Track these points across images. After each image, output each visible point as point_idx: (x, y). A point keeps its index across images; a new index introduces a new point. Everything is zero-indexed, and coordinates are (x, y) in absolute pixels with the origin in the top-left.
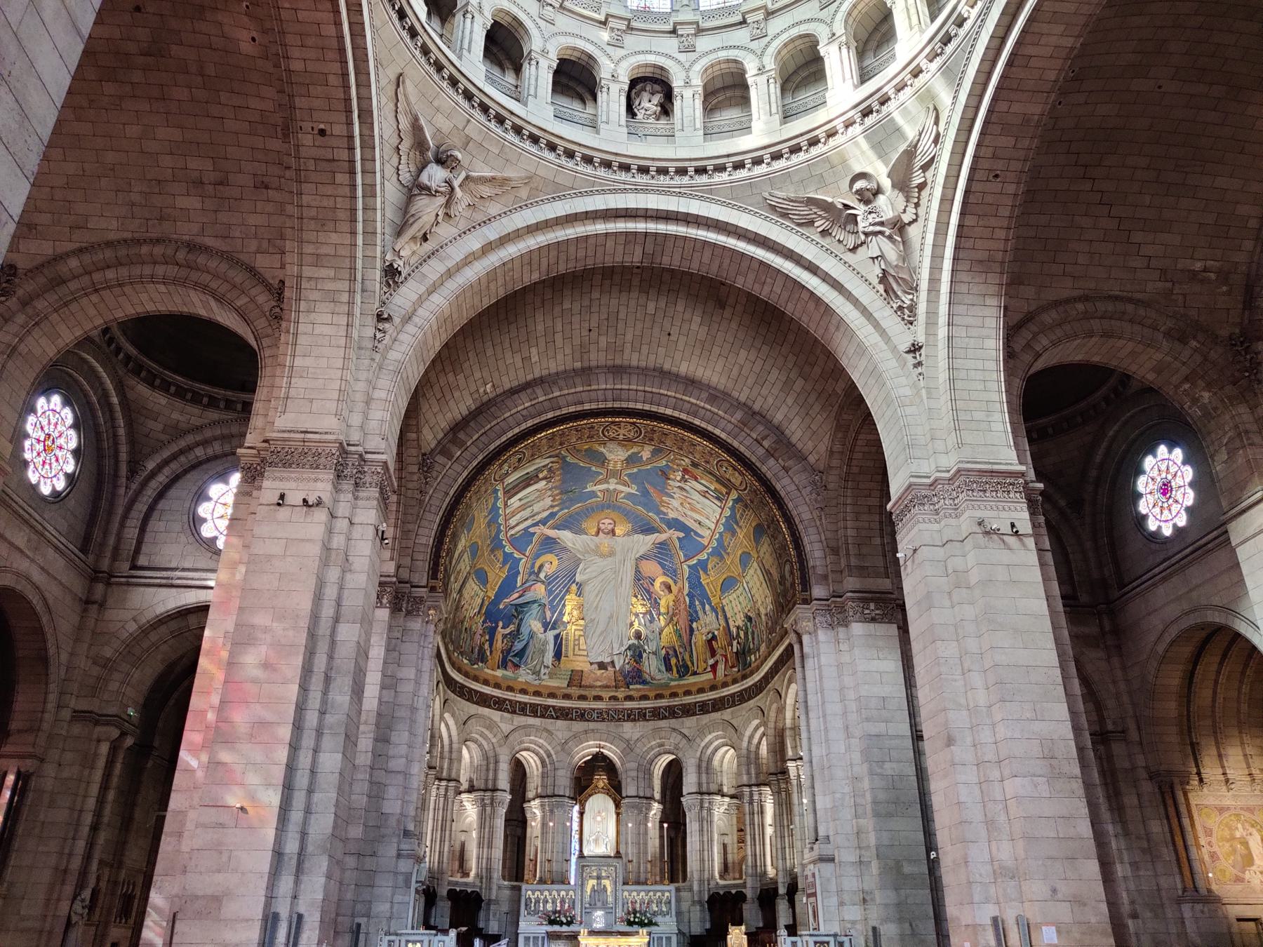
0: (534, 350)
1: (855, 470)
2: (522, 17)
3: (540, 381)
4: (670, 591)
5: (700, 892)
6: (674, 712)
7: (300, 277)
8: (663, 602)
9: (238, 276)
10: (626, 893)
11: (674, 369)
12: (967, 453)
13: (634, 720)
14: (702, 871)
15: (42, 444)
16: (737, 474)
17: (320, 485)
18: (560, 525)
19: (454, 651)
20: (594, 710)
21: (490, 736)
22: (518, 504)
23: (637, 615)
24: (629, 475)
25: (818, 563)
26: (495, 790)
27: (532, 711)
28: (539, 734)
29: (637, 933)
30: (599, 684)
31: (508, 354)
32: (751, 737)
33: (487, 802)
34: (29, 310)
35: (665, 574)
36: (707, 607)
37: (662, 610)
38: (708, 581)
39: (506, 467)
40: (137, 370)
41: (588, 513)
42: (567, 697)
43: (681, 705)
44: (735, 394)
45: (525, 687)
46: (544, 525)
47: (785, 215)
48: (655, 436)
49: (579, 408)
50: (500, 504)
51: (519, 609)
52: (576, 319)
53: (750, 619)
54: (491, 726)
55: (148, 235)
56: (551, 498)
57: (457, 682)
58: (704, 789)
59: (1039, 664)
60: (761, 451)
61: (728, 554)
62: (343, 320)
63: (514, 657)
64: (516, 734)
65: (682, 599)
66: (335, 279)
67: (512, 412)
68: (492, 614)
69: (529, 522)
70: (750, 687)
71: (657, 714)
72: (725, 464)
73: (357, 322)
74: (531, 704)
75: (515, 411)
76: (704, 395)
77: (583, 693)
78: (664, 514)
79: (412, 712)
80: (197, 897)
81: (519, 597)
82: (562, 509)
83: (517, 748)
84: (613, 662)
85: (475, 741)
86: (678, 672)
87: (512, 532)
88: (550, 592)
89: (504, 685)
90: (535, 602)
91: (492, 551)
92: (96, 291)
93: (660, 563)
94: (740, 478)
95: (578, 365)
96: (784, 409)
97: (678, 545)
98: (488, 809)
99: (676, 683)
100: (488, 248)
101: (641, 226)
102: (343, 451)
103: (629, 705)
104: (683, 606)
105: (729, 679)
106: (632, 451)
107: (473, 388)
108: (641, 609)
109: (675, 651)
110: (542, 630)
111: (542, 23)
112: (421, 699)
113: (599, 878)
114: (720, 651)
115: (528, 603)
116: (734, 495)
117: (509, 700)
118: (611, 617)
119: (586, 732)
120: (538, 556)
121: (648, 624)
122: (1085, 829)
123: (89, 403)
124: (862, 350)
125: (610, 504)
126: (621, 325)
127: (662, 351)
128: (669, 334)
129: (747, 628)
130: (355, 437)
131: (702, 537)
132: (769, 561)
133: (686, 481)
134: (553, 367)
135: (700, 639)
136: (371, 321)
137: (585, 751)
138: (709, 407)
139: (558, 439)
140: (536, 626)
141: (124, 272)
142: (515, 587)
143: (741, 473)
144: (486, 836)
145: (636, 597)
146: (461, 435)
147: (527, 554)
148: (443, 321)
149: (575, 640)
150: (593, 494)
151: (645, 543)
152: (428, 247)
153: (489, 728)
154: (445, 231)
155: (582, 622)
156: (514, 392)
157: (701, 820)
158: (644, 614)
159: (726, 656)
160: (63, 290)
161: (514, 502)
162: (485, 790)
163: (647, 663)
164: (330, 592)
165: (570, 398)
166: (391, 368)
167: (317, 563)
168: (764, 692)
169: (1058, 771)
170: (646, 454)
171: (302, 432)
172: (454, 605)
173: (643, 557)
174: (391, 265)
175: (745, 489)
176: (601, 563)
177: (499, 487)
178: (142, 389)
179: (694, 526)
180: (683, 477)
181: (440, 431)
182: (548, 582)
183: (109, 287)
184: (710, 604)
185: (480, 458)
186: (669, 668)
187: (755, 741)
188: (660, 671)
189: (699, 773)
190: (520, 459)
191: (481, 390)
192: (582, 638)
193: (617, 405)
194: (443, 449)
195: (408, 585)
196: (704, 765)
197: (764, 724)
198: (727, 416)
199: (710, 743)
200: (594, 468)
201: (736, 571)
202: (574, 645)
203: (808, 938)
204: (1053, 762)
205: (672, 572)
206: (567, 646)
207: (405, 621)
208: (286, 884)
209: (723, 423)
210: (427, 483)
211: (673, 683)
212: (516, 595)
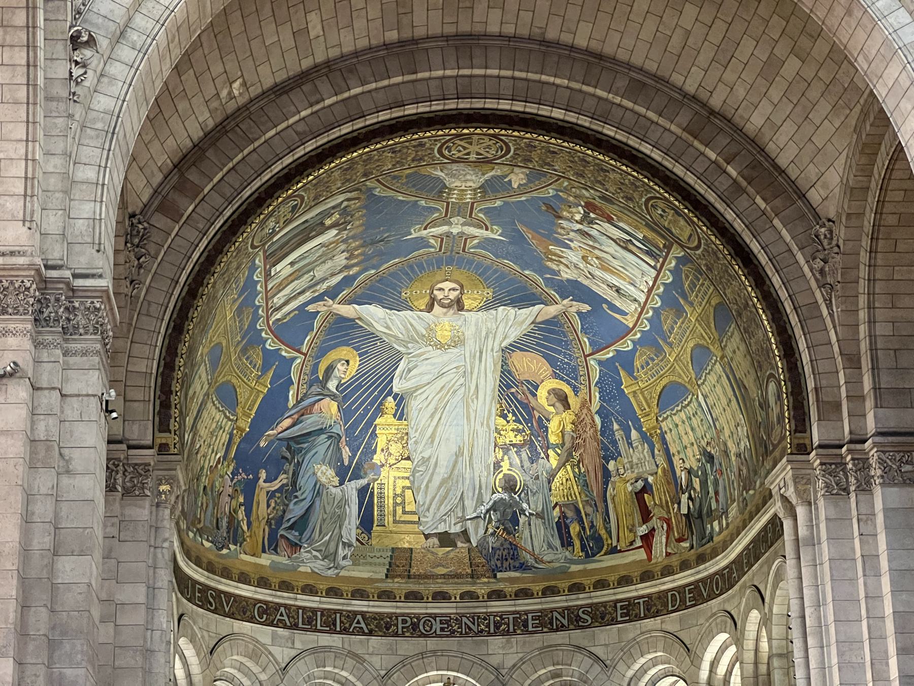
0: (313, 18)
1: (891, 220)
3: (327, 68)
8: (553, 426)
11: (566, 38)
13: (507, 633)
16: (682, 222)
17: (11, 341)
18: (360, 297)
19: (188, 528)
20: (434, 616)
21: (256, 669)
22: (289, 270)
23: (506, 449)
24: (487, 211)
25: (824, 383)
28: (340, 663)
30: (442, 571)
32: (714, 664)
35: (556, 376)
36: (634, 434)
37: (553, 439)
38: (636, 388)
39: (271, 223)
41: (412, 273)
42: (386, 595)
43: (590, 605)
44: (677, 79)
45: (311, 582)
46: (333, 298)
48: (535, 156)
49: (397, 113)
50: (258, 276)
51: (294, 446)
53: (710, 458)
54: (257, 652)
57: (196, 582)
60: (723, 184)
61: (670, 345)
62: (20, 57)
64: (300, 664)
65: (588, 420)
67: (280, 128)
69: (308, 295)
70: (711, 577)
72: (660, 204)
74: (323, 611)
75: (284, 125)
77: (413, 587)
79: (145, 658)
81: (293, 425)
82: (366, 270)
84: (465, 533)
86: (583, 547)
87: (278, 316)
88: (346, 413)
89: (275, 581)
90: (321, 431)
93: (546, 356)
94: (688, 231)
95: (392, 36)
96: (765, 108)
99: (580, 567)
102: (44, 283)
103: (497, 606)
104: (590, 432)
105: (675, 561)
107: (210, 91)
108: (511, 437)
109: (578, 511)
110: (336, 480)
112: (157, 634)
114: (657, 512)
115: (309, 434)
116: (676, 252)
117: (286, 606)
118: (459, 454)
119: (422, 655)
120: (323, 352)
121: (527, 464)
124: (890, 51)
129: (705, 473)
130: (56, 253)
131: (623, 313)
132: (742, 365)
133: (591, 222)
136: (61, 49)
138: (630, 105)
139: (360, 169)
140: (326, 474)
142: (287, 409)
143: (690, 222)
145: (505, 417)
146: (193, 176)
150: (422, 243)
153: (254, 656)
155: (407, 464)
156: (280, 90)
159: (668, 521)
161: (283, 268)
163: (526, 533)
165: (380, 97)
166: (99, 125)
167: (21, 469)
168: (736, 587)
173: (515, 346)
175: (698, 247)
176: (437, 358)
177: (261, 253)
179: (609, 295)
180: (585, 219)
181: (156, 170)
182: (345, 394)
184: (639, 429)
185: (227, 213)
186: (566, 542)
187: (721, 670)
188: (550, 546)
191: (224, 93)
192: (408, 493)
193: (464, 104)
195: (124, 447)
197: (738, 641)
198: (661, 121)
200: (423, 203)
201: (685, 374)
202: (396, 504)
206: (381, 507)
209: (654, 135)
210: (140, 266)
211: (574, 568)
212: (287, 423)
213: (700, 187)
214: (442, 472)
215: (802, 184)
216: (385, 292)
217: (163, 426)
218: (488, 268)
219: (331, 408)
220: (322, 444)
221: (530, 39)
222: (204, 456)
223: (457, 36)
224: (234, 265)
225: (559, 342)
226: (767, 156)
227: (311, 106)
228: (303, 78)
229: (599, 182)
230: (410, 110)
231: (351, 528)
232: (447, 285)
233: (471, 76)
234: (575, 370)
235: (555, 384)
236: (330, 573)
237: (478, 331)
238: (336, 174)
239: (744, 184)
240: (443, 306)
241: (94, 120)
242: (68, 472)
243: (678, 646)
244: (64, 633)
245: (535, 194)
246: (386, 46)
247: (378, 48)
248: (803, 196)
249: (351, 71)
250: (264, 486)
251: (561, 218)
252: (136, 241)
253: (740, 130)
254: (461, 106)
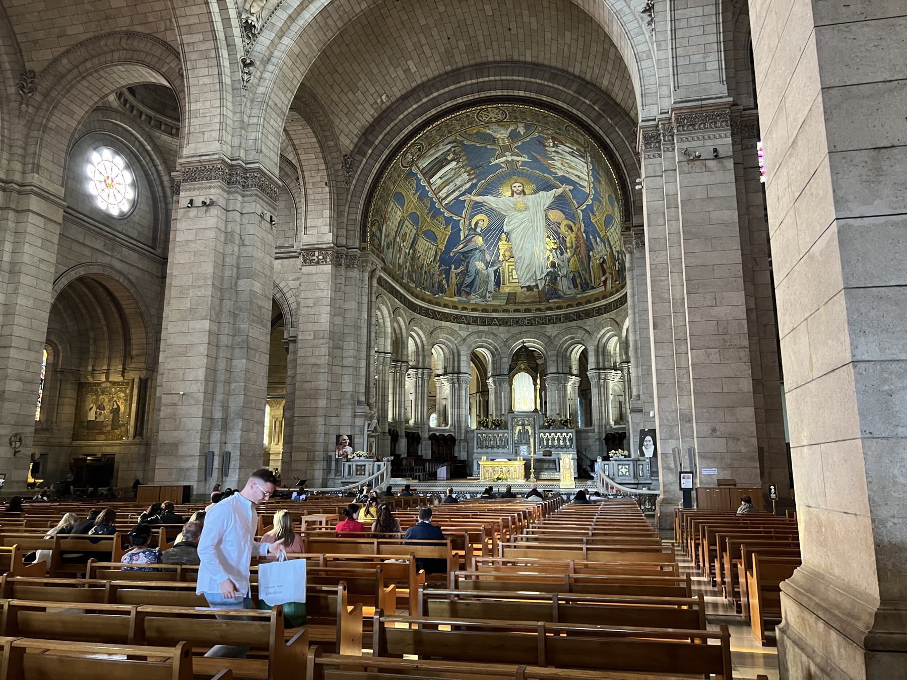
0: (410, 62)
4: (572, 231)
5: (599, 433)
6: (580, 316)
7: (182, 44)
8: (568, 239)
9: (158, 51)
10: (542, 434)
11: (522, 59)
12: (682, 94)
13: (553, 323)
14: (601, 419)
15: (103, 184)
17: (212, 191)
18: (482, 192)
19: (416, 287)
20: (525, 318)
21: (453, 340)
22: (439, 182)
26: (459, 373)
27: (482, 322)
28: (488, 337)
29: (516, 460)
30: (528, 300)
31: (391, 70)
33: (456, 380)
34: (49, 99)
35: (567, 219)
36: (598, 239)
37: (568, 245)
40: (159, 125)
44: (571, 70)
46: (470, 194)
50: (423, 183)
51: (465, 255)
52: (435, 32)
54: (453, 333)
55: (103, 32)
56: (466, 174)
58: (601, 366)
59: (723, 262)
64: (471, 338)
66: (203, 41)
68: (445, 260)
71: (568, 318)
72: (570, 129)
73: (227, 70)
74: (480, 317)
76: (547, 75)
77: (517, 307)
78: (556, 173)
80: (165, 444)
82: (479, 181)
83: (474, 346)
84: (537, 285)
85: (444, 344)
86: (582, 288)
87: (446, 202)
88: (486, 241)
89: (460, 306)
90: (477, 249)
91: (433, 217)
92: (84, 78)
93: (561, 211)
95: (449, 68)
96: (607, 76)
97: (571, 195)
98: (456, 385)
104: (582, 241)
105: (614, 290)
106: (510, 129)
107: (372, 101)
109: (579, 273)
110: (485, 268)
113: (523, 425)
114: (608, 271)
117: (465, 316)
119: (520, 333)
120: (472, 217)
121: (559, 256)
122: (746, 385)
123: (132, 152)
125: (513, 172)
126: (471, 30)
127: (508, 44)
128: (510, 29)
133: (557, 146)
134: (430, 73)
135: (595, 263)
137: (517, 345)
141: (96, 61)
144: (456, 401)
145: (549, 238)
146: (370, 138)
147: (463, 216)
148: (296, 58)
149: (509, 273)
150: (498, 166)
151: (547, 197)
156: (404, 98)
157: (599, 387)
158: (556, 249)
159: (612, 274)
160: (64, 82)
162: (453, 374)
166: (259, 100)
169: (729, 343)
170: (522, 130)
171: (200, 156)
172: (409, 258)
173: (550, 208)
174: (247, 21)
176: (520, 216)
178: (165, 137)
179: (576, 179)
180: (554, 143)
181: (354, 136)
182: (485, 233)
183: (91, 74)
184: (599, 237)
186: (575, 286)
188: (569, 288)
189: (597, 356)
190: (419, 149)
191: (379, 101)
193: (482, 95)
194: (359, 150)
196: (600, 350)
199: (604, 335)
202: (509, 276)
203: (614, 462)
204: (727, 337)
205: (571, 216)
206: (504, 277)
207: (346, 272)
208: (216, 436)
210: (350, 176)
211: (579, 296)
212: (461, 246)
213: (584, 118)
214: (527, 262)
215: (627, 109)
216: (492, 190)
217: (363, 239)
218: (530, 175)
219: (479, 240)
220: (477, 254)
221: (507, 61)
222: (424, 260)
223: (476, 65)
224: (395, 175)
225: (565, 204)
226: (612, 99)
227: (416, 103)
228: (413, 91)
229: (546, 123)
230: (460, 100)
231: (492, 286)
232: (517, 185)
233: (484, 82)
234: (573, 215)
235: (566, 222)
236: (484, 303)
237: (534, 203)
238: (434, 132)
239: (602, 113)
240: (518, 194)
241: (257, 98)
242: (243, 245)
243: (615, 324)
244: (240, 310)
245: (531, 136)
246: (447, 73)
247: (443, 75)
248: (628, 115)
249: (433, 86)
250: (454, 271)
251: (546, 146)
252: (348, 166)
253: (599, 89)
254: (481, 96)
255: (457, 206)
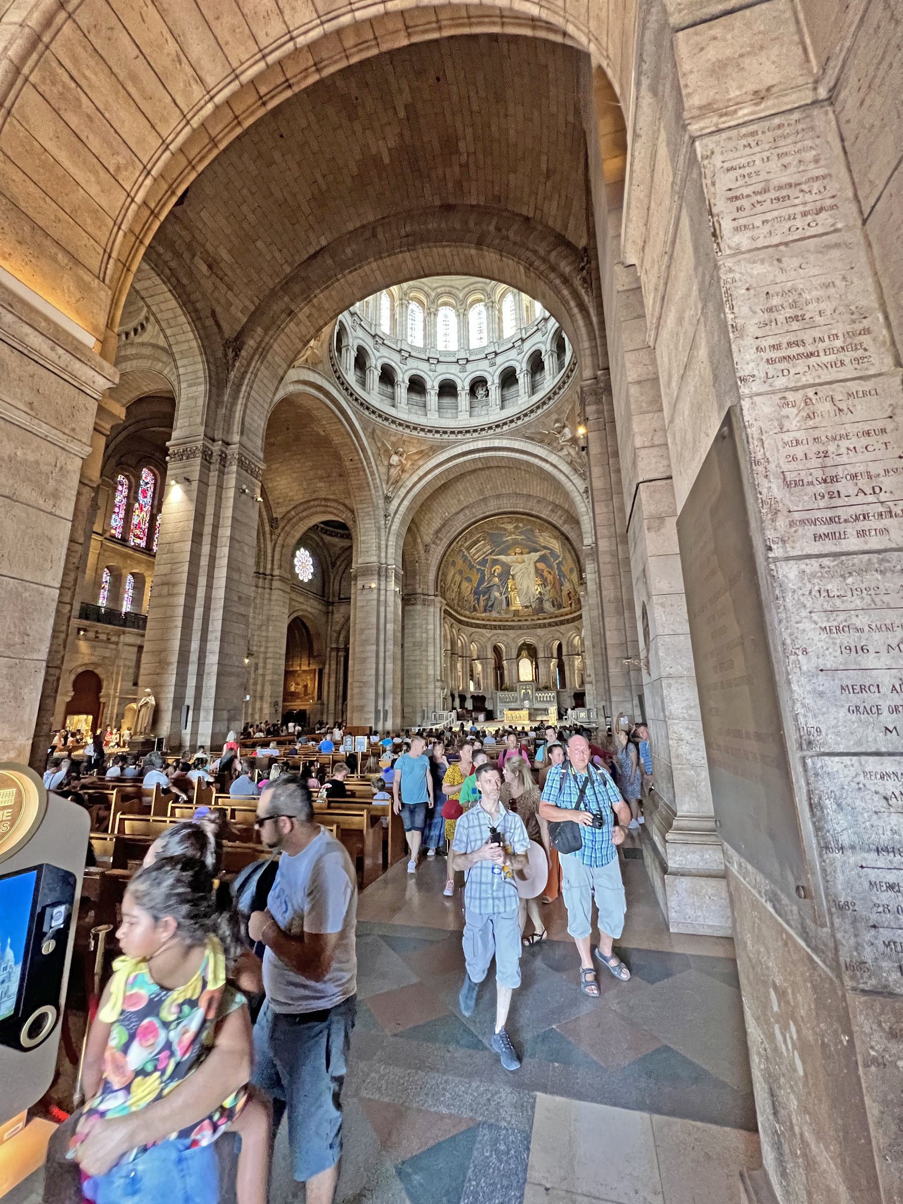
2: (422, 374)
9: (341, 507)
47: (532, 439)
63: (488, 608)
68: (476, 593)
71: (550, 625)
100: (420, 479)
101: (477, 455)
102: (380, 568)
111: (431, 373)
135: (565, 593)
140: (497, 594)
151: (535, 556)
152: (400, 484)
154: (405, 476)
161: (473, 551)
164: (382, 615)
176: (521, 566)
182: (499, 576)
205: (550, 566)
231: (504, 606)
250: (482, 598)
255: (484, 562)
